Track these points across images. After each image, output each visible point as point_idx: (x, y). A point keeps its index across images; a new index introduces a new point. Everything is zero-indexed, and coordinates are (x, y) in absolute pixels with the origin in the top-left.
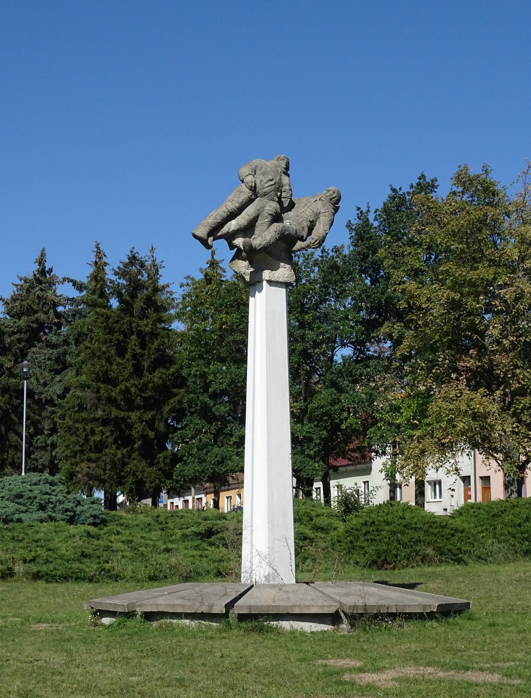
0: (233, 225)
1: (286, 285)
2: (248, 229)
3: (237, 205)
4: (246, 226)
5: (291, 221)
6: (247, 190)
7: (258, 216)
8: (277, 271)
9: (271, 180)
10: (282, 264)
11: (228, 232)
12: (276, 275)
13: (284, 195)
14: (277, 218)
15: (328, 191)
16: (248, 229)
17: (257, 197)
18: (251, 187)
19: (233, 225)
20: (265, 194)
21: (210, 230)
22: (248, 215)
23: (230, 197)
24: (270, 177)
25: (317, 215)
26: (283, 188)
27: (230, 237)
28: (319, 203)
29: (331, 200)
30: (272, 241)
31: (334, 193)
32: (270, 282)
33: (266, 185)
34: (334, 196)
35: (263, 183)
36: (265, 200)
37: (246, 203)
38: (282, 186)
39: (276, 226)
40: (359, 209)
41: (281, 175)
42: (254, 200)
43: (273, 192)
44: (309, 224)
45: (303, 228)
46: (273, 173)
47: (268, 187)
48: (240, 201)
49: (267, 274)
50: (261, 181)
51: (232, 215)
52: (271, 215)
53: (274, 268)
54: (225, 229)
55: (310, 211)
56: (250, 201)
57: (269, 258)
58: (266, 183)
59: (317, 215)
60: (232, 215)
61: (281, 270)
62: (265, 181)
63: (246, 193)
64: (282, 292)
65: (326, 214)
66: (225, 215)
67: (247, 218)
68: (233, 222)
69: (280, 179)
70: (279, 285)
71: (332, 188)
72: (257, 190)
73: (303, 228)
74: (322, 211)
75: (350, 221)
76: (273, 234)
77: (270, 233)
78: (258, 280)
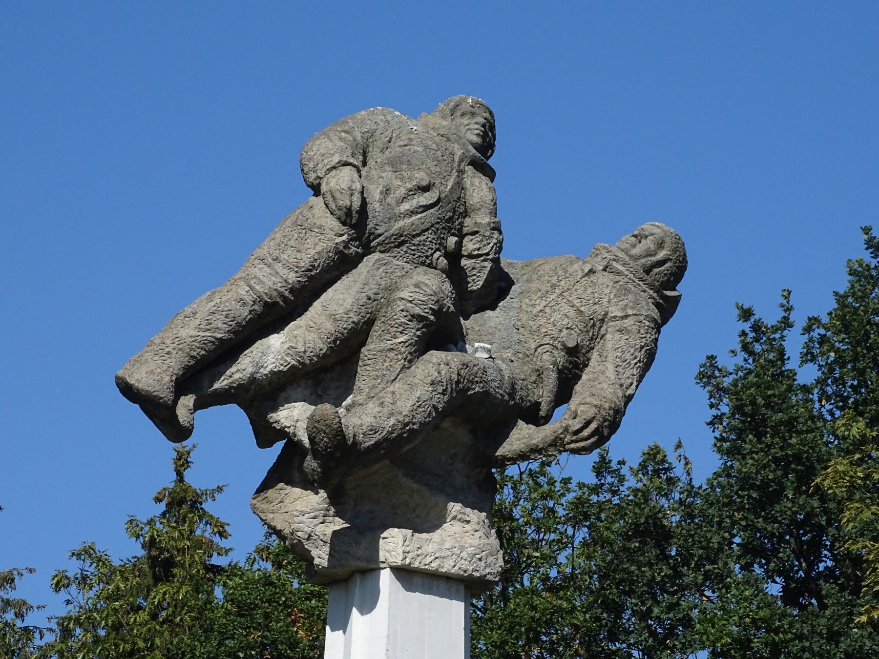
0: (272, 353)
2: (330, 372)
3: (292, 277)
5: (494, 345)
6: (332, 223)
7: (370, 323)
8: (436, 535)
9: (426, 189)
10: (455, 508)
11: (252, 380)
12: (430, 548)
13: (469, 245)
14: (440, 332)
15: (640, 238)
16: (330, 372)
17: (368, 250)
18: (349, 211)
19: (272, 353)
20: (400, 241)
21: (187, 369)
22: (332, 317)
23: (266, 248)
24: (421, 177)
25: (595, 327)
26: (468, 221)
27: (259, 399)
28: (604, 279)
29: (648, 271)
30: (419, 418)
31: (661, 245)
32: (408, 575)
33: (405, 206)
34: (661, 255)
36: (397, 262)
37: (327, 269)
38: (465, 214)
39: (438, 364)
40: (746, 314)
41: (461, 172)
43: (430, 235)
44: (560, 357)
45: (539, 373)
46: (430, 163)
47: (413, 213)
49: (394, 545)
50: (387, 191)
51: (273, 315)
52: (420, 318)
53: (424, 522)
54: (243, 368)
55: (566, 309)
56: (340, 265)
58: (404, 199)
59: (595, 327)
60: (273, 315)
61: (450, 531)
62: (403, 191)
63: (327, 235)
64: (451, 614)
65: (629, 322)
66: (244, 313)
67: (329, 326)
69: (459, 186)
70: (443, 585)
71: (655, 228)
73: (539, 373)
74: (615, 311)
75: (711, 358)
76: (422, 391)
77: (412, 386)
78: (363, 565)
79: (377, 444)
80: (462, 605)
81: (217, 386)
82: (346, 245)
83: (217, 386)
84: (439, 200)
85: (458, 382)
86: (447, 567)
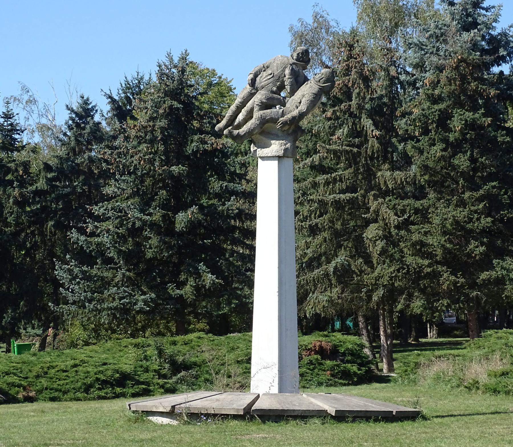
0: (240, 117)
1: (279, 158)
3: (240, 100)
4: (246, 116)
6: (248, 87)
9: (271, 74)
10: (273, 142)
14: (265, 106)
17: (257, 91)
21: (227, 122)
24: (270, 72)
29: (319, 81)
30: (252, 127)
32: (263, 158)
33: (265, 79)
35: (261, 79)
37: (248, 97)
38: (285, 76)
41: (286, 67)
42: (255, 94)
43: (271, 84)
46: (275, 68)
48: (242, 96)
50: (261, 77)
56: (251, 95)
57: (264, 138)
61: (273, 146)
68: (241, 114)
69: (284, 71)
72: (256, 85)
79: (245, 134)
80: (277, 162)
81: (235, 124)
82: (251, 91)
83: (235, 124)
84: (273, 76)
85: (261, 117)
86: (269, 155)
